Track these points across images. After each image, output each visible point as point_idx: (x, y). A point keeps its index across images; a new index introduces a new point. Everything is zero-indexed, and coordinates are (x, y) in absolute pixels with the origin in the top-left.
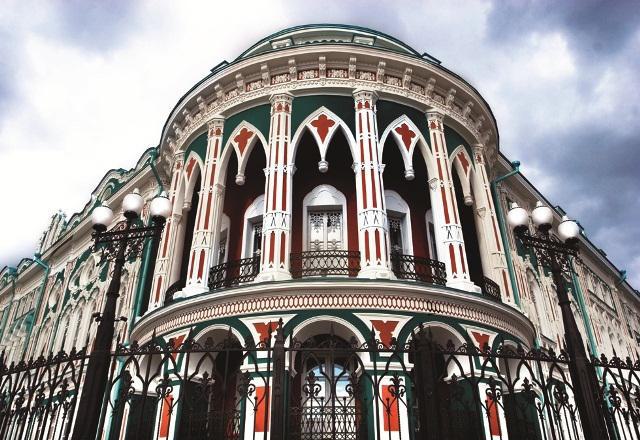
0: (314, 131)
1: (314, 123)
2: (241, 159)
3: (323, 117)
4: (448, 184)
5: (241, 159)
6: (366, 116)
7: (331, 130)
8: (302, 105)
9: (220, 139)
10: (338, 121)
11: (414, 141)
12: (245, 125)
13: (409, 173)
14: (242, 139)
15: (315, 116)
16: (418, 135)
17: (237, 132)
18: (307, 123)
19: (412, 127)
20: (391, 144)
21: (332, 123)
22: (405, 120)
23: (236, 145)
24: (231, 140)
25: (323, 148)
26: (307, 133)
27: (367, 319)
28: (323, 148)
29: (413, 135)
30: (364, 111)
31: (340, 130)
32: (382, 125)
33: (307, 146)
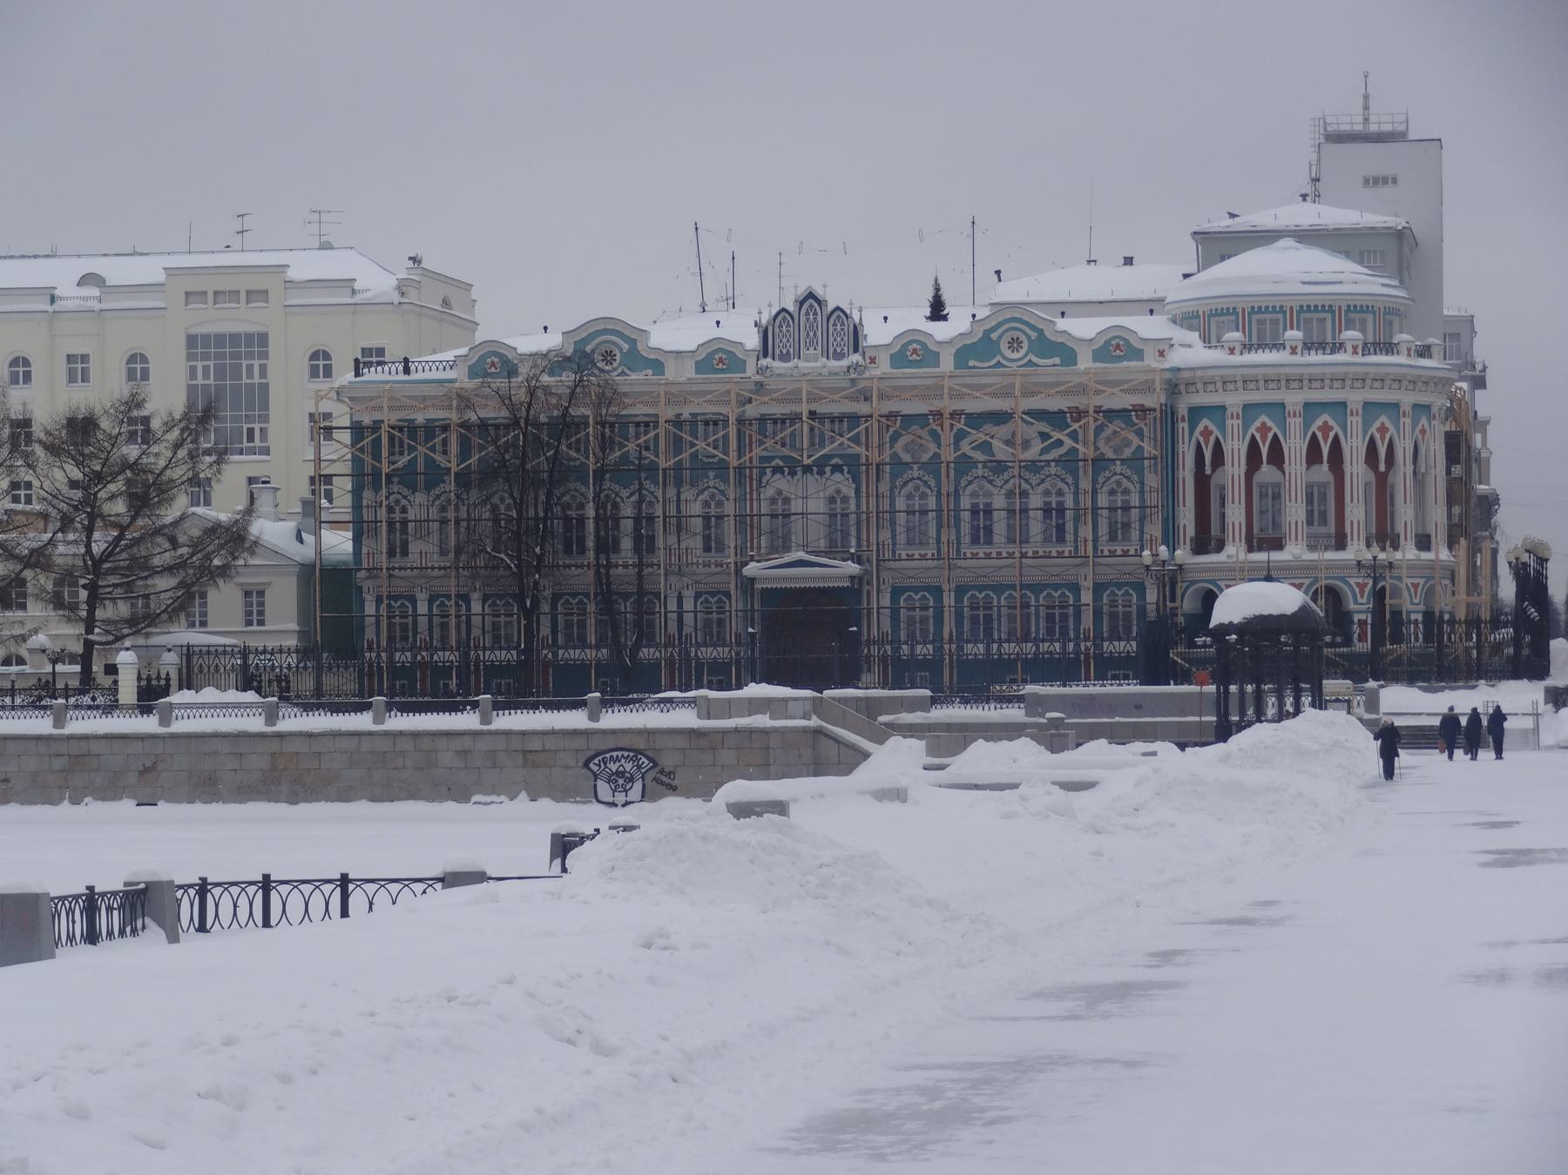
0: (1319, 435)
1: (1319, 428)
2: (1264, 451)
4: (1410, 468)
5: (1264, 451)
7: (1332, 435)
8: (1311, 409)
10: (1337, 429)
11: (1388, 436)
12: (1264, 418)
13: (1382, 468)
14: (1264, 429)
15: (1319, 422)
17: (1258, 424)
18: (1314, 428)
20: (1372, 442)
21: (1331, 428)
22: (1383, 419)
23: (1258, 436)
24: (1252, 430)
25: (1325, 450)
28: (1325, 450)
29: (1387, 430)
30: (1354, 419)
31: (1336, 437)
32: (1366, 425)
33: (1314, 446)
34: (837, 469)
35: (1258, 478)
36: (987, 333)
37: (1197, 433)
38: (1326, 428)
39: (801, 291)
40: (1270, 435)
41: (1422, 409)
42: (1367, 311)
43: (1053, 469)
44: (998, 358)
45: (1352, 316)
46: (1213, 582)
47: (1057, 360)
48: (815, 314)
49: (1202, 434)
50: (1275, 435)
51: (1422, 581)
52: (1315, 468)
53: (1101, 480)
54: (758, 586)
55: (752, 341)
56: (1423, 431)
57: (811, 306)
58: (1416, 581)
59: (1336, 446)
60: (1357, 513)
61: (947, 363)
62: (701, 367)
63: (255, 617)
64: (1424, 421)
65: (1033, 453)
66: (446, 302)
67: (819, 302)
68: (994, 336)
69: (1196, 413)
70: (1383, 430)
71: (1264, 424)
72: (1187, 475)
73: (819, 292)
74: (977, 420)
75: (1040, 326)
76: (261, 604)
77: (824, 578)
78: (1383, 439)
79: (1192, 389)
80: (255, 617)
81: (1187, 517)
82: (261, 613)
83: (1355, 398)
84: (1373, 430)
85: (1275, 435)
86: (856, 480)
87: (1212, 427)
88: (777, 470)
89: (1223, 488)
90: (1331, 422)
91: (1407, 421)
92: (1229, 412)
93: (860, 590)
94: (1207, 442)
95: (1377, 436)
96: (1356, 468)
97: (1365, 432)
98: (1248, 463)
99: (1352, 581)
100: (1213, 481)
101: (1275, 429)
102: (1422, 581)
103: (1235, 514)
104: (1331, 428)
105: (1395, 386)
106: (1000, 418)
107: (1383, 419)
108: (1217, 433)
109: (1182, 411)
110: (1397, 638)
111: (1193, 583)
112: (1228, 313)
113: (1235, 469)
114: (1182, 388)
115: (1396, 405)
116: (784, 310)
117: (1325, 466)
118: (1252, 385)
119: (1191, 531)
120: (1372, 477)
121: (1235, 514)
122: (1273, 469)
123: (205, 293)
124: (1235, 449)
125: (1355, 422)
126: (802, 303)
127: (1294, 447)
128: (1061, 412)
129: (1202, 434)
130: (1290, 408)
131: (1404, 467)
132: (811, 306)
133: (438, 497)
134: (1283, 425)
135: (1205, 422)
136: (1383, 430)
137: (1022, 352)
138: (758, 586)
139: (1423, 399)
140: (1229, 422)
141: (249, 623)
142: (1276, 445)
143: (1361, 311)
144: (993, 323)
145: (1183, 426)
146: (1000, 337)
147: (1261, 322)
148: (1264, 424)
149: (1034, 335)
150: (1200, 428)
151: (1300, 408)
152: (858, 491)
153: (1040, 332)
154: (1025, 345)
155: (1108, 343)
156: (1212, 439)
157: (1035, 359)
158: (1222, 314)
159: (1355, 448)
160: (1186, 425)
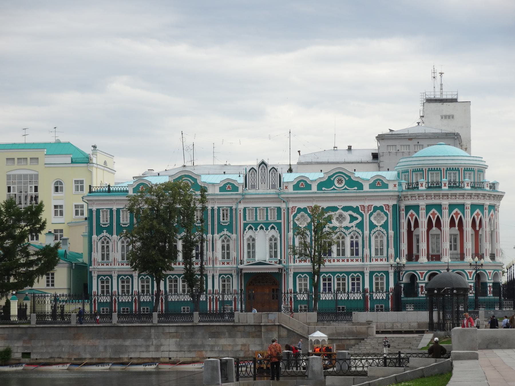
0: (454, 216)
1: (454, 214)
2: (434, 222)
3: (457, 212)
5: (434, 222)
6: (468, 211)
7: (459, 216)
8: (452, 207)
9: (425, 211)
10: (461, 214)
13: (478, 228)
15: (454, 211)
16: (481, 215)
17: (431, 212)
18: (452, 213)
19: (480, 212)
21: (459, 214)
22: (478, 210)
23: (431, 216)
24: (429, 214)
25: (457, 222)
26: (452, 216)
28: (457, 222)
31: (461, 217)
34: (273, 228)
35: (431, 232)
36: (330, 177)
37: (408, 215)
38: (457, 214)
39: (259, 161)
40: (436, 216)
42: (472, 170)
44: (334, 187)
45: (465, 172)
46: (415, 271)
47: (356, 188)
48: (265, 170)
49: (410, 215)
50: (438, 217)
51: (492, 271)
52: (453, 228)
53: (372, 232)
54: (243, 272)
55: (241, 180)
56: (492, 215)
57: (263, 167)
58: (490, 271)
59: (461, 220)
60: (469, 245)
61: (314, 188)
62: (222, 189)
63: (50, 283)
64: (492, 211)
65: (346, 223)
66: (105, 163)
67: (266, 165)
68: (332, 179)
69: (408, 208)
70: (478, 214)
71: (434, 212)
72: (404, 230)
73: (266, 161)
75: (349, 175)
76: (53, 278)
77: (269, 269)
78: (478, 218)
79: (406, 199)
80: (50, 283)
81: (404, 247)
82: (53, 281)
83: (468, 202)
84: (474, 214)
85: (438, 217)
86: (280, 233)
87: (414, 213)
88: (250, 228)
89: (418, 236)
90: (459, 212)
91: (487, 211)
92: (420, 207)
93: (281, 273)
94: (412, 219)
95: (476, 217)
96: (468, 229)
97: (471, 215)
98: (428, 227)
99: (467, 271)
100: (414, 233)
101: (438, 214)
102: (492, 271)
103: (423, 246)
104: (459, 214)
106: (335, 209)
107: (478, 210)
108: (416, 215)
109: (403, 207)
110: (485, 294)
111: (407, 271)
112: (420, 171)
113: (423, 228)
114: (403, 198)
115: (483, 205)
116: (253, 168)
117: (457, 228)
118: (429, 198)
119: (406, 252)
120: (473, 233)
121: (423, 246)
122: (437, 229)
123: (14, 159)
124: (423, 221)
126: (260, 165)
127: (446, 221)
128: (357, 207)
129: (410, 215)
130: (443, 206)
132: (263, 167)
133: (101, 238)
134: (441, 212)
135: (412, 211)
136: (478, 214)
137: (343, 185)
138: (243, 272)
140: (420, 212)
141: (48, 285)
142: (438, 221)
143: (469, 170)
144: (332, 174)
145: (403, 213)
146: (334, 179)
148: (434, 212)
149: (347, 179)
150: (410, 213)
151: (447, 206)
152: (281, 237)
153: (349, 177)
154: (344, 182)
155: (375, 181)
156: (414, 218)
158: (417, 171)
159: (468, 221)
160: (404, 212)
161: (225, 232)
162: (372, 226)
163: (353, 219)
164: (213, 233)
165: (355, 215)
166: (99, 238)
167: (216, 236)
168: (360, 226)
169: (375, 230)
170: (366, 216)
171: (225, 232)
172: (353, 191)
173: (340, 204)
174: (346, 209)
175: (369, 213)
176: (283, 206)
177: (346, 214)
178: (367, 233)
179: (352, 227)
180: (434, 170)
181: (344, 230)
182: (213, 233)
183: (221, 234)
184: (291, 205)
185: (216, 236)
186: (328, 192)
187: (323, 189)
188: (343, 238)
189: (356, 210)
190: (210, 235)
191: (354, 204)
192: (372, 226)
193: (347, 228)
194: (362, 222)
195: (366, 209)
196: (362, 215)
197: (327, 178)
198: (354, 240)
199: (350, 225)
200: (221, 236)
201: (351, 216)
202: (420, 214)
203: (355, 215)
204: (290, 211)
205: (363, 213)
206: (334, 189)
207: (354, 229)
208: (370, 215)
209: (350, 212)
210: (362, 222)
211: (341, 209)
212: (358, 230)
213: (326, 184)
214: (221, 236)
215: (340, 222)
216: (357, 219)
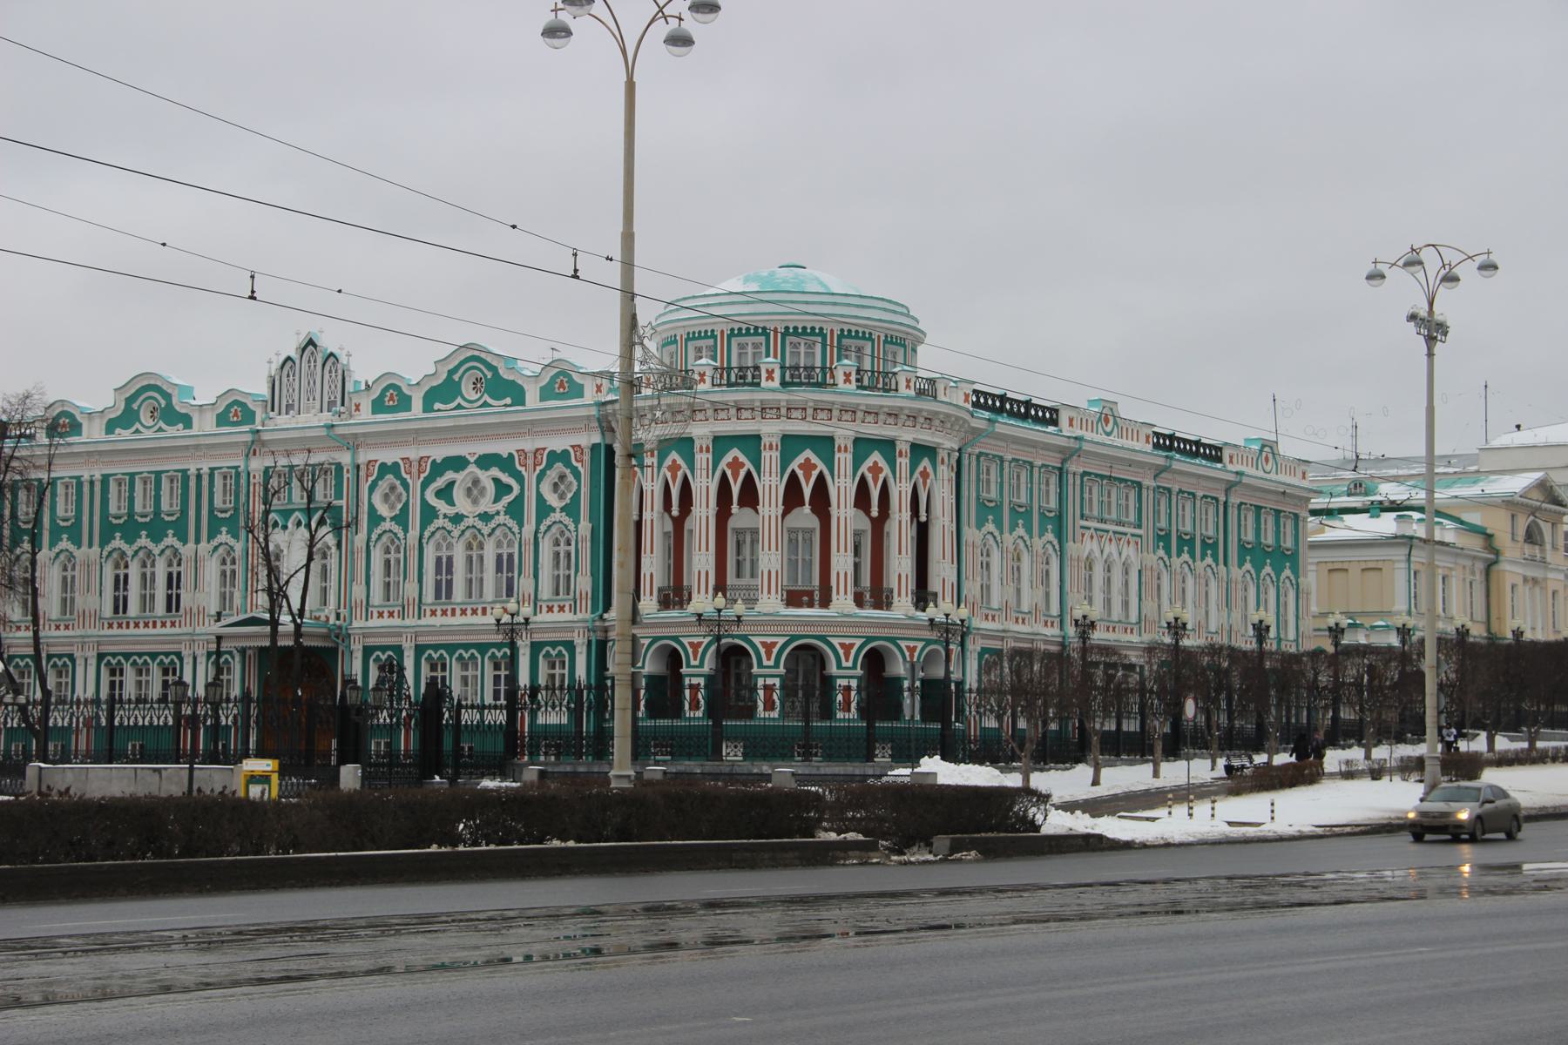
27: (835, 642)
36: (451, 373)
41: (920, 451)
43: (501, 519)
44: (459, 400)
45: (845, 341)
47: (508, 401)
59: (821, 486)
65: (486, 505)
68: (456, 377)
74: (438, 468)
96: (844, 512)
105: (890, 420)
106: (458, 463)
120: (866, 525)
125: (844, 459)
131: (900, 516)
139: (925, 437)
147: (741, 346)
157: (490, 401)
161: (224, 537)
162: (544, 509)
163: (502, 489)
164: (198, 541)
165: (505, 478)
166: (53, 555)
167: (204, 547)
168: (515, 510)
169: (548, 522)
170: (530, 478)
171: (224, 537)
172: (500, 410)
173: (471, 449)
174: (485, 461)
175: (539, 468)
176: (345, 458)
177: (486, 477)
178: (529, 529)
179: (498, 513)
180: (748, 333)
181: (479, 524)
182: (198, 541)
183: (215, 543)
184: (363, 458)
185: (204, 547)
186: (445, 414)
187: (437, 406)
188: (481, 546)
189: (506, 463)
190: (191, 545)
191: (503, 448)
192: (544, 509)
193: (485, 517)
194: (520, 497)
195: (530, 462)
196: (520, 478)
197: (445, 376)
198: (505, 551)
199: (491, 509)
200: (216, 548)
201: (496, 481)
202: (698, 465)
203: (505, 478)
204: (362, 473)
205: (522, 469)
206: (459, 407)
207: (501, 519)
208: (540, 478)
209: (495, 472)
210: (520, 497)
211: (476, 462)
212: (512, 523)
213: (443, 391)
214: (216, 548)
215: (475, 502)
216: (509, 489)
